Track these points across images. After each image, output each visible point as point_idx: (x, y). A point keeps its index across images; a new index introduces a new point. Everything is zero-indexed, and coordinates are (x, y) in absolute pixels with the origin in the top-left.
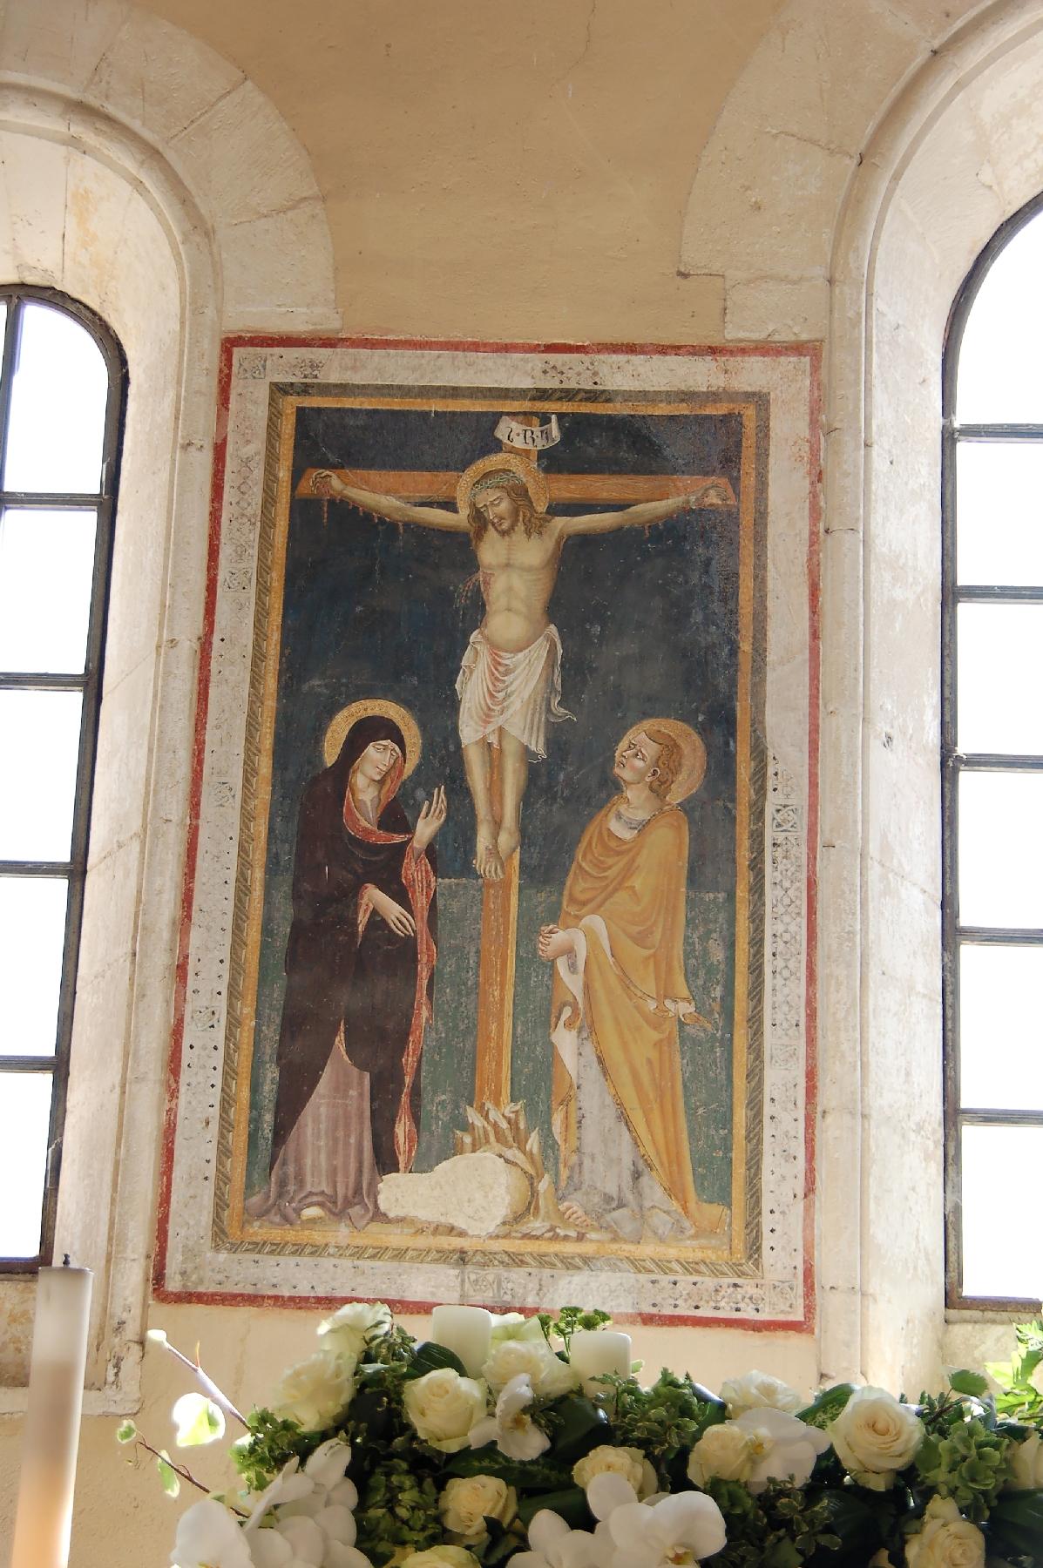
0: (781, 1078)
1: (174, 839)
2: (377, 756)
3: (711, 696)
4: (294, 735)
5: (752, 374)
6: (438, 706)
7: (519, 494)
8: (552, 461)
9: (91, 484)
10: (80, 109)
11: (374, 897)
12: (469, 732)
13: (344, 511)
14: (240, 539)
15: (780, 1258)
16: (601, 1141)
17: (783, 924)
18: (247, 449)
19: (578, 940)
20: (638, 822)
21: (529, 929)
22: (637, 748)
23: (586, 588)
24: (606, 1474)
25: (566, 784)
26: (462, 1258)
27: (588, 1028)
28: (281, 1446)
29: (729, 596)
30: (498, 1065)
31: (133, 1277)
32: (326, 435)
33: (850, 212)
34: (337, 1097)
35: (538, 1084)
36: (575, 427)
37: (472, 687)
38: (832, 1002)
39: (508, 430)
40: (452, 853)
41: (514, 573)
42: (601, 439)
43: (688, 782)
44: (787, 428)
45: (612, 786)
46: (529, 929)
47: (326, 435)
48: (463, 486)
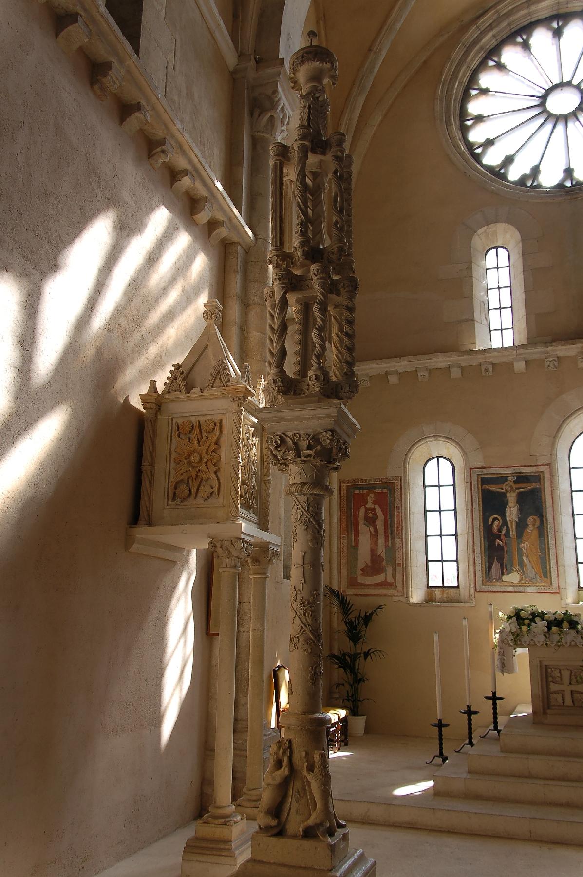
0: (553, 562)
1: (471, 534)
2: (496, 523)
3: (539, 512)
5: (541, 469)
6: (503, 516)
7: (511, 487)
8: (515, 482)
9: (452, 483)
10: (447, 438)
11: (498, 540)
12: (508, 519)
13: (489, 491)
14: (475, 495)
15: (555, 584)
16: (530, 571)
17: (552, 542)
18: (475, 483)
19: (525, 546)
20: (531, 529)
21: (518, 545)
22: (530, 520)
23: (522, 499)
24: (537, 619)
25: (521, 525)
26: (514, 586)
27: (527, 556)
28: (509, 618)
29: (541, 499)
30: (516, 562)
31: (472, 590)
32: (485, 480)
33: (553, 445)
34: (496, 566)
35: (521, 564)
36: (518, 477)
37: (508, 513)
38: (559, 552)
39: (509, 479)
40: (507, 535)
41: (512, 498)
43: (538, 524)
44: (547, 475)
45: (527, 525)
46: (518, 545)
47: (485, 480)
48: (504, 486)
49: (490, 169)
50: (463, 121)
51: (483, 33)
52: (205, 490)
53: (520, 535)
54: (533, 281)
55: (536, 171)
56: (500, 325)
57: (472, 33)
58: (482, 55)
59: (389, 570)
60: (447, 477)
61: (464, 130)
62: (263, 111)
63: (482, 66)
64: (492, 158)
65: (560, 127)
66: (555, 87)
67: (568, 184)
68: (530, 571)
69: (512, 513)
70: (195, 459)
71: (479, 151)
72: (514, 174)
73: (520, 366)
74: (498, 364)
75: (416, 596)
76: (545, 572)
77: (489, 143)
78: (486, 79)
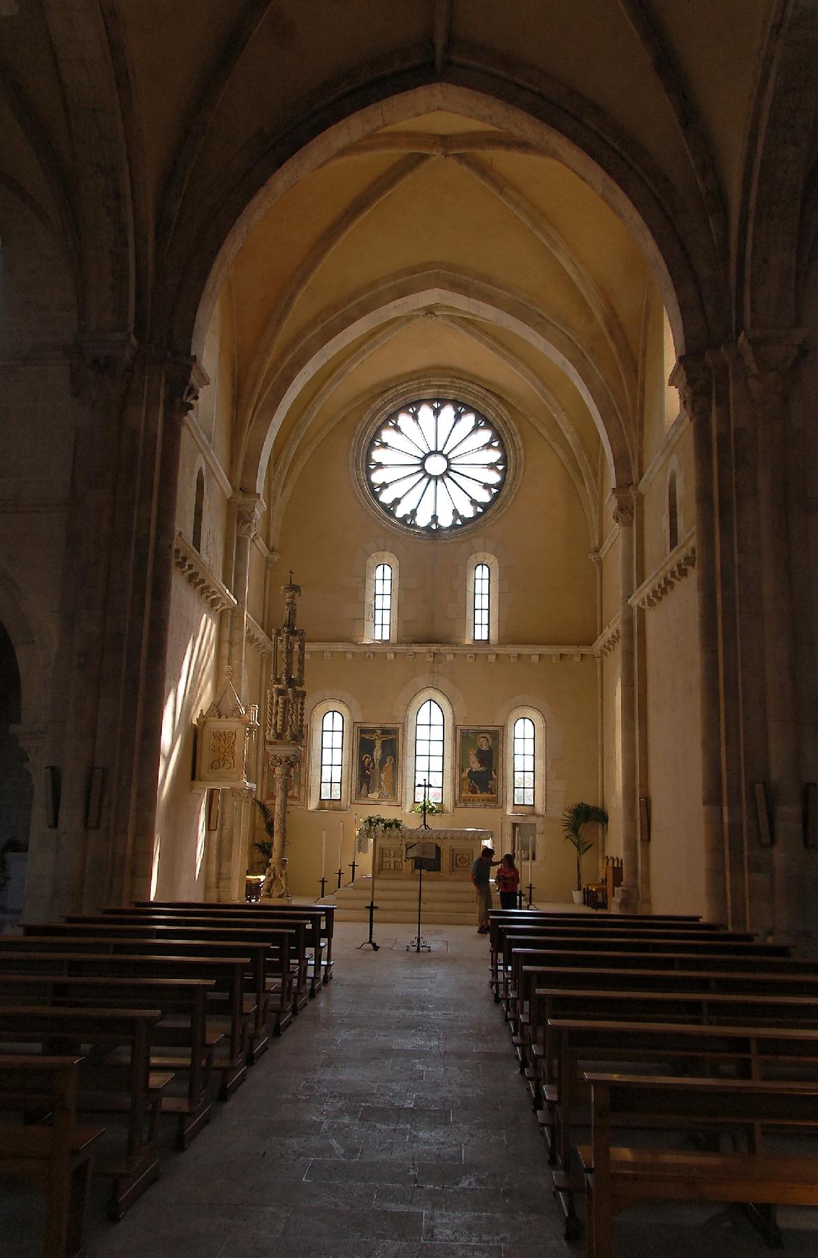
4: (360, 758)
6: (372, 756)
19: (383, 776)
23: (385, 745)
25: (382, 762)
35: (380, 787)
41: (378, 743)
42: (385, 731)
47: (363, 731)
49: (383, 505)
51: (386, 403)
52: (227, 765)
53: (381, 769)
54: (405, 596)
55: (414, 513)
57: (379, 403)
58: (385, 417)
59: (296, 790)
60: (338, 726)
61: (369, 472)
62: (246, 522)
63: (384, 425)
64: (386, 497)
66: (431, 453)
67: (434, 527)
68: (385, 791)
69: (377, 753)
70: (222, 750)
72: (400, 512)
75: (313, 805)
76: (395, 794)
77: (384, 486)
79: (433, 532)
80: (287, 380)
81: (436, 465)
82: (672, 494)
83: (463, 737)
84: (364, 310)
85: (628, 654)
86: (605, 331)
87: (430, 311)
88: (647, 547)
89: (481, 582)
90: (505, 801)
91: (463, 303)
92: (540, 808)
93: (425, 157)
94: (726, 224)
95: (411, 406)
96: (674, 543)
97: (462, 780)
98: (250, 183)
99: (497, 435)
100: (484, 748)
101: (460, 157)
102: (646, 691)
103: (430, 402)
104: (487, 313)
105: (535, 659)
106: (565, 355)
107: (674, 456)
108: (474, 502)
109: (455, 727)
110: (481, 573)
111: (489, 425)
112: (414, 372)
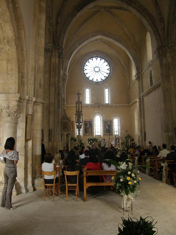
20: (90, 128)
23: (89, 124)
25: (89, 127)
33: (93, 117)
34: (86, 133)
35: (89, 132)
42: (89, 122)
50: (83, 69)
54: (92, 95)
56: (88, 100)
57: (85, 57)
65: (96, 72)
67: (97, 81)
71: (86, 74)
73: (90, 106)
74: (87, 106)
76: (92, 134)
77: (87, 73)
78: (87, 63)
79: (97, 83)
80: (72, 53)
81: (97, 69)
82: (151, 74)
83: (104, 122)
84: (87, 39)
85: (140, 105)
86: (134, 44)
87: (96, 40)
88: (144, 85)
89: (107, 91)
90: (113, 134)
91: (105, 38)
92: (119, 135)
93: (100, 11)
94: (164, 25)
95: (91, 58)
96: (151, 85)
97: (105, 130)
98: (72, 15)
99: (108, 64)
100: (109, 124)
101: (107, 11)
102: (144, 112)
103: (95, 57)
104: (110, 40)
105: (118, 106)
106: (126, 48)
107: (151, 67)
108: (105, 77)
109: (103, 120)
110: (107, 91)
111: (107, 62)
112: (92, 51)
